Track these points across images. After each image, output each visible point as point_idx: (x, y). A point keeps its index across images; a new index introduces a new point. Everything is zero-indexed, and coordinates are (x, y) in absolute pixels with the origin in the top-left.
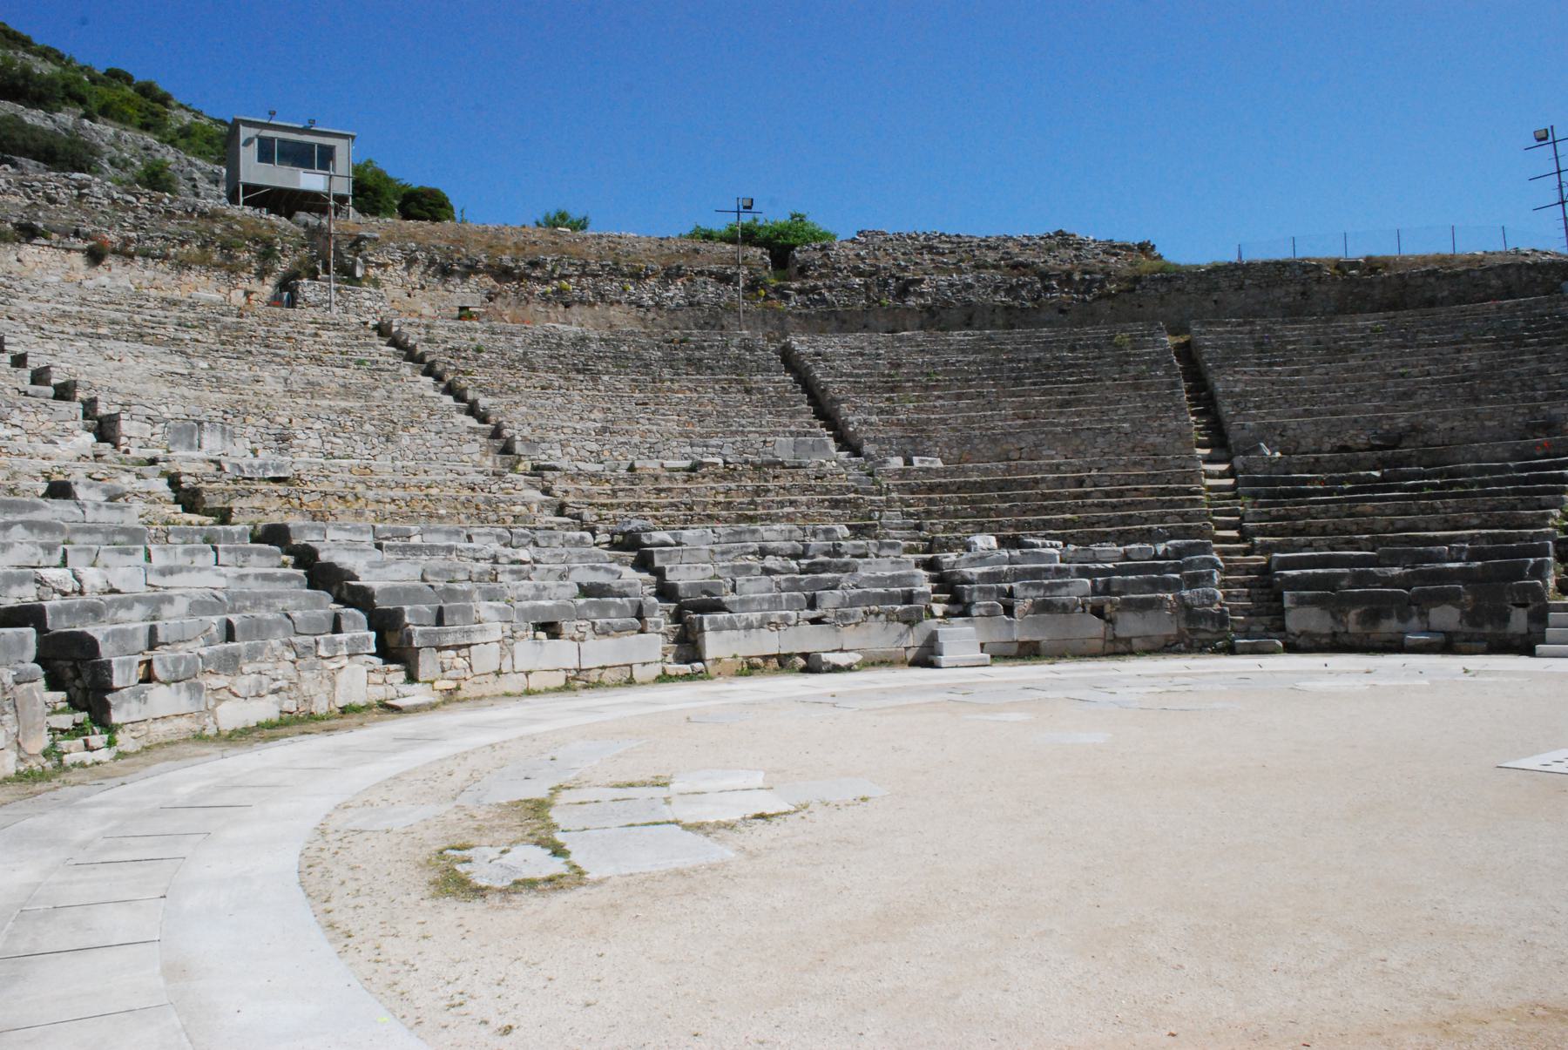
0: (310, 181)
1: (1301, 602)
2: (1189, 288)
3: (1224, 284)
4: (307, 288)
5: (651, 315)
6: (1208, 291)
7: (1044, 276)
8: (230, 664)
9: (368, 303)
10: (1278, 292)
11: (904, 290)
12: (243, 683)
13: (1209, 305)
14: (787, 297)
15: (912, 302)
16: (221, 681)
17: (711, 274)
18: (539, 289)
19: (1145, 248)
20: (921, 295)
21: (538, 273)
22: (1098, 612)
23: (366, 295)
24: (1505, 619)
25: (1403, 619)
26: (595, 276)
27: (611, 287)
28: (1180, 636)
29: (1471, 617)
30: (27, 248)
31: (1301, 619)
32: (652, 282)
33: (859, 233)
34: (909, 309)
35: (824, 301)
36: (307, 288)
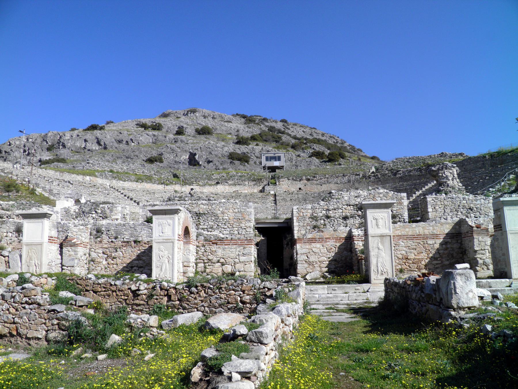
0: (276, 164)
3: (466, 164)
4: (267, 188)
6: (462, 166)
10: (478, 164)
11: (395, 174)
14: (370, 178)
15: (398, 176)
18: (315, 182)
19: (461, 154)
20: (400, 174)
21: (315, 179)
33: (397, 159)
34: (397, 178)
35: (378, 178)
36: (267, 188)
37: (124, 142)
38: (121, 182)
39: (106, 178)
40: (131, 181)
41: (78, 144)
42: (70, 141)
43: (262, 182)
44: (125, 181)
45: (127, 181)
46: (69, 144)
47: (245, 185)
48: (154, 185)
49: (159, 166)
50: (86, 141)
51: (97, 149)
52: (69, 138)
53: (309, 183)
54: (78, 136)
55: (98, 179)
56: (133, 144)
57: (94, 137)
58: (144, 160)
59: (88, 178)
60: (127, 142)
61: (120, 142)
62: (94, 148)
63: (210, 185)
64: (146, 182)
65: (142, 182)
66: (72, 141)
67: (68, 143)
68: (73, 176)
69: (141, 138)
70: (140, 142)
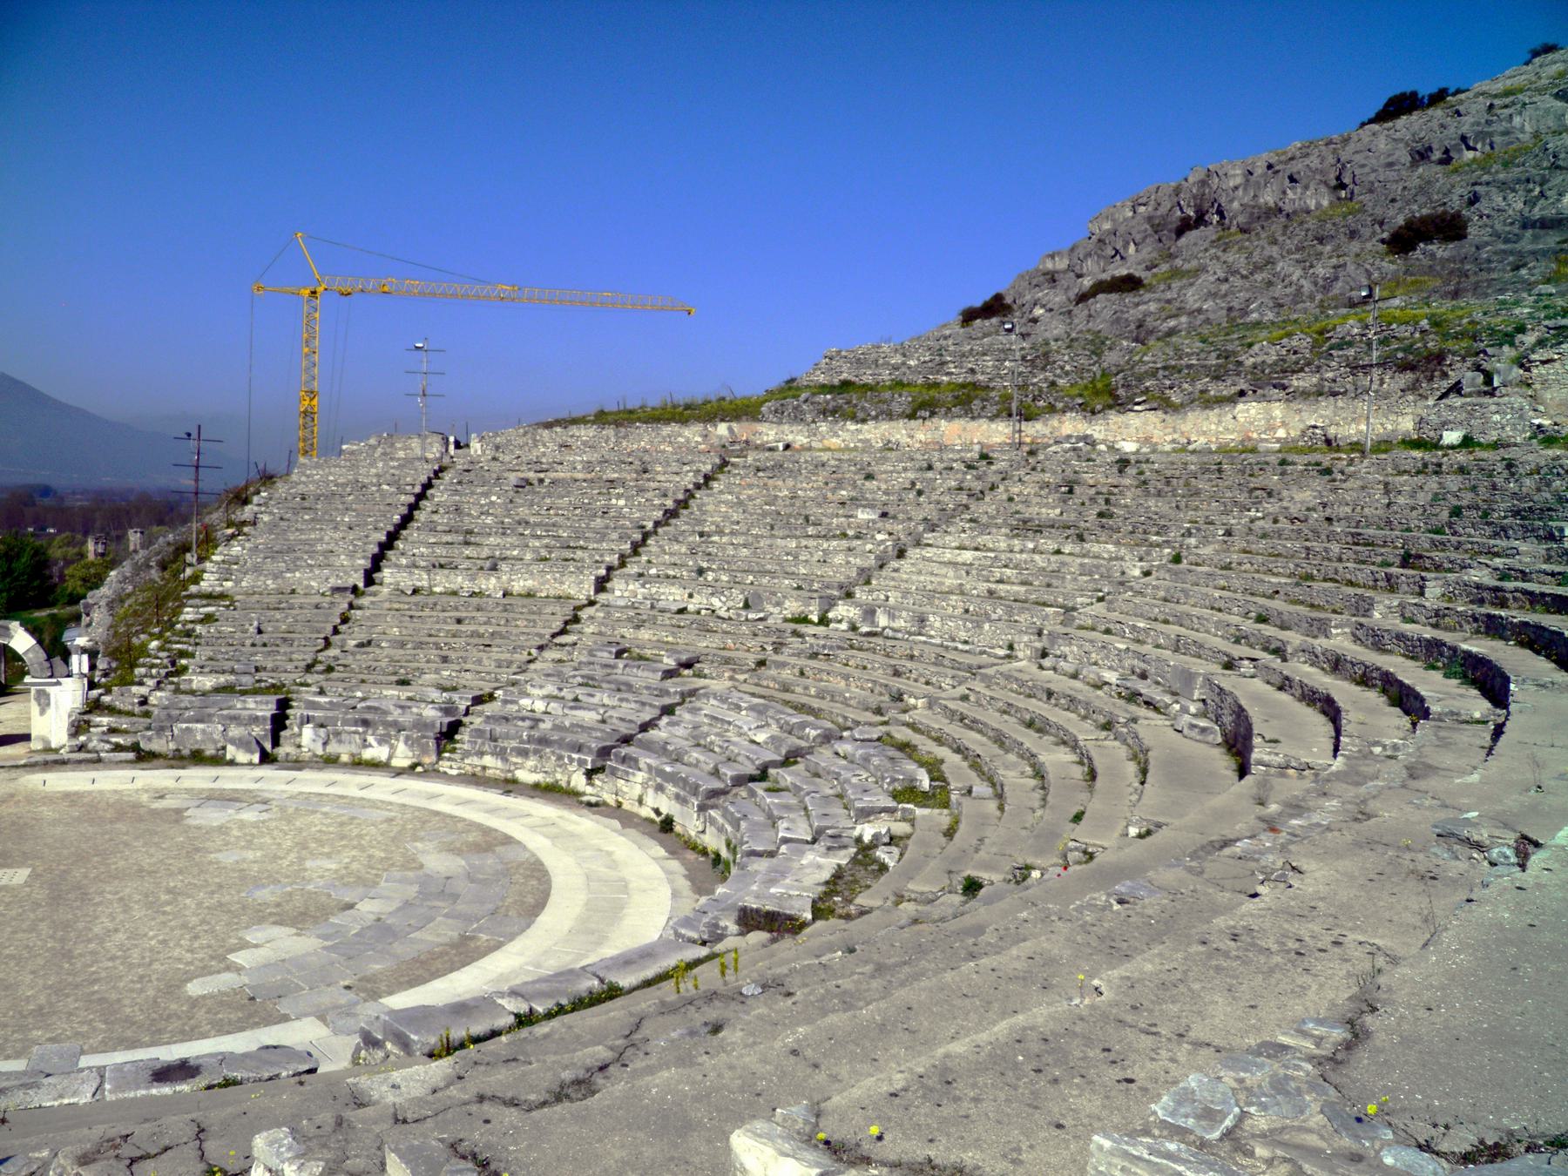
8: (524, 753)
9: (1497, 417)
12: (531, 763)
16: (519, 760)
23: (1493, 408)
30: (1240, 406)
37: (1437, 155)
38: (851, 426)
39: (797, 418)
40: (890, 416)
41: (1268, 198)
42: (1240, 192)
43: (1445, 375)
44: (864, 421)
45: (876, 418)
46: (1236, 205)
47: (1360, 393)
48: (974, 424)
49: (1433, 255)
50: (1292, 179)
51: (1325, 203)
52: (1239, 180)
54: (1270, 167)
55: (762, 427)
56: (1470, 155)
57: (1331, 160)
58: (1383, 241)
59: (722, 429)
60: (1447, 151)
61: (1421, 155)
62: (1312, 204)
63: (1209, 403)
64: (949, 415)
65: (933, 414)
66: (1245, 189)
67: (1231, 201)
68: (666, 430)
69: (1517, 120)
70: (1497, 139)
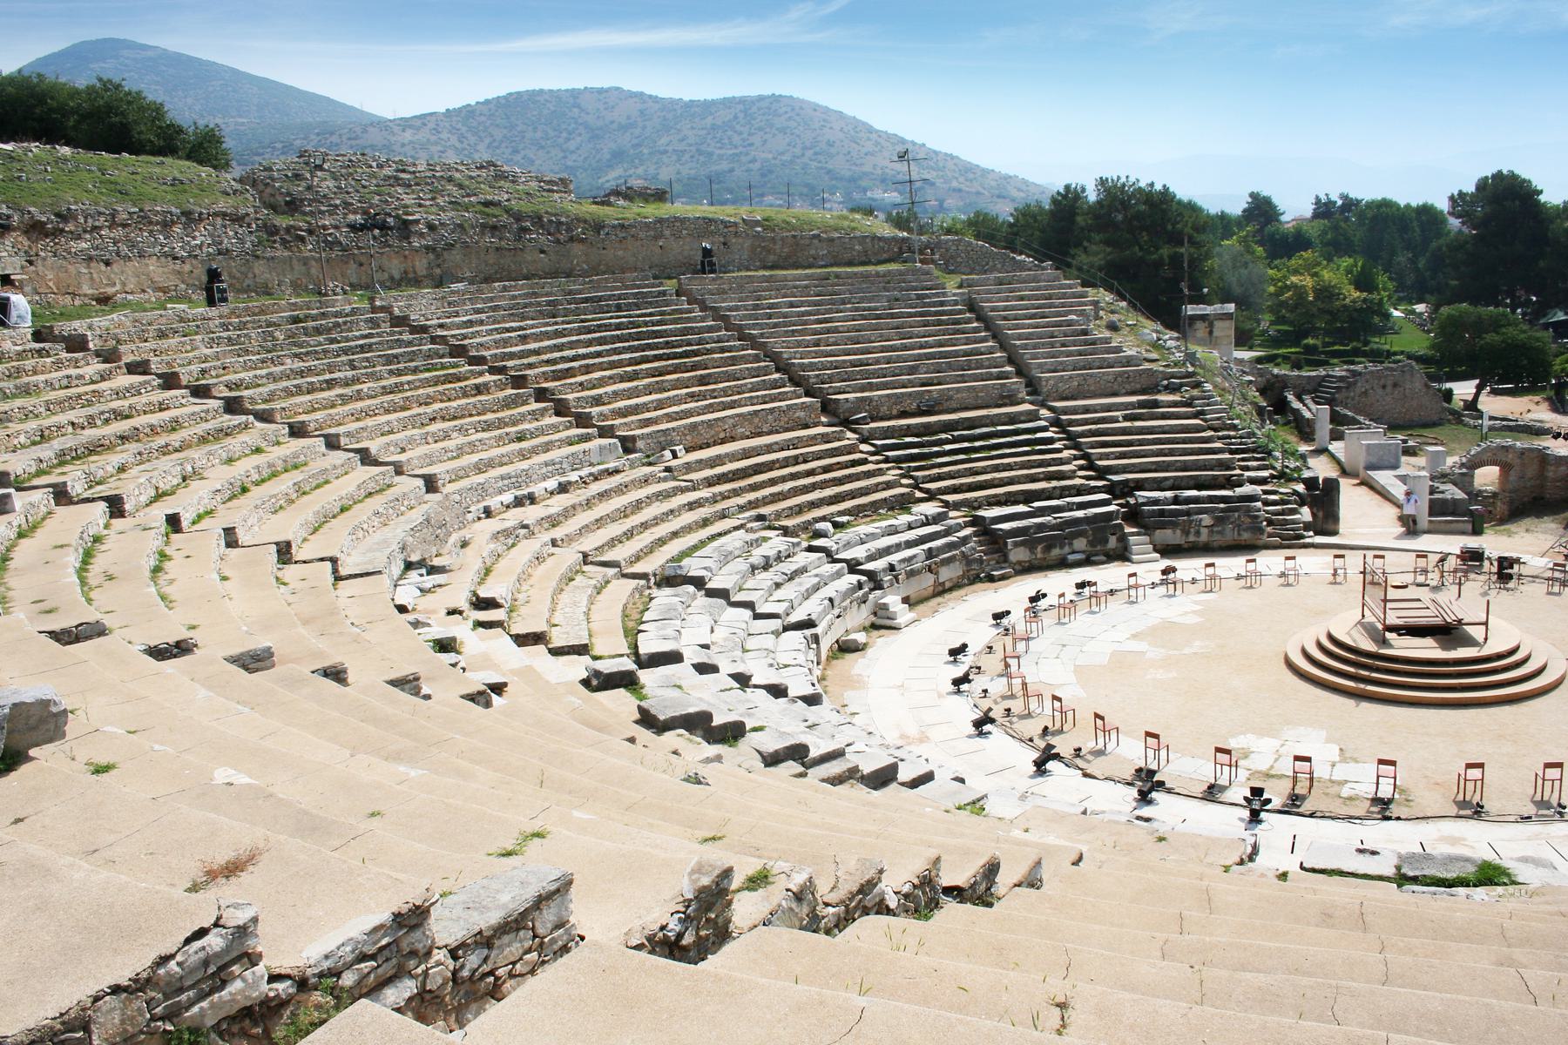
1: (1016, 545)
2: (642, 235)
3: (667, 233)
5: (187, 267)
6: (656, 238)
7: (518, 217)
13: (658, 251)
17: (224, 215)
21: (70, 227)
22: (930, 570)
24: (1107, 541)
25: (1062, 547)
26: (124, 226)
27: (142, 237)
28: (963, 576)
29: (1091, 543)
31: (1018, 555)
32: (177, 229)
53: (43, 247)
